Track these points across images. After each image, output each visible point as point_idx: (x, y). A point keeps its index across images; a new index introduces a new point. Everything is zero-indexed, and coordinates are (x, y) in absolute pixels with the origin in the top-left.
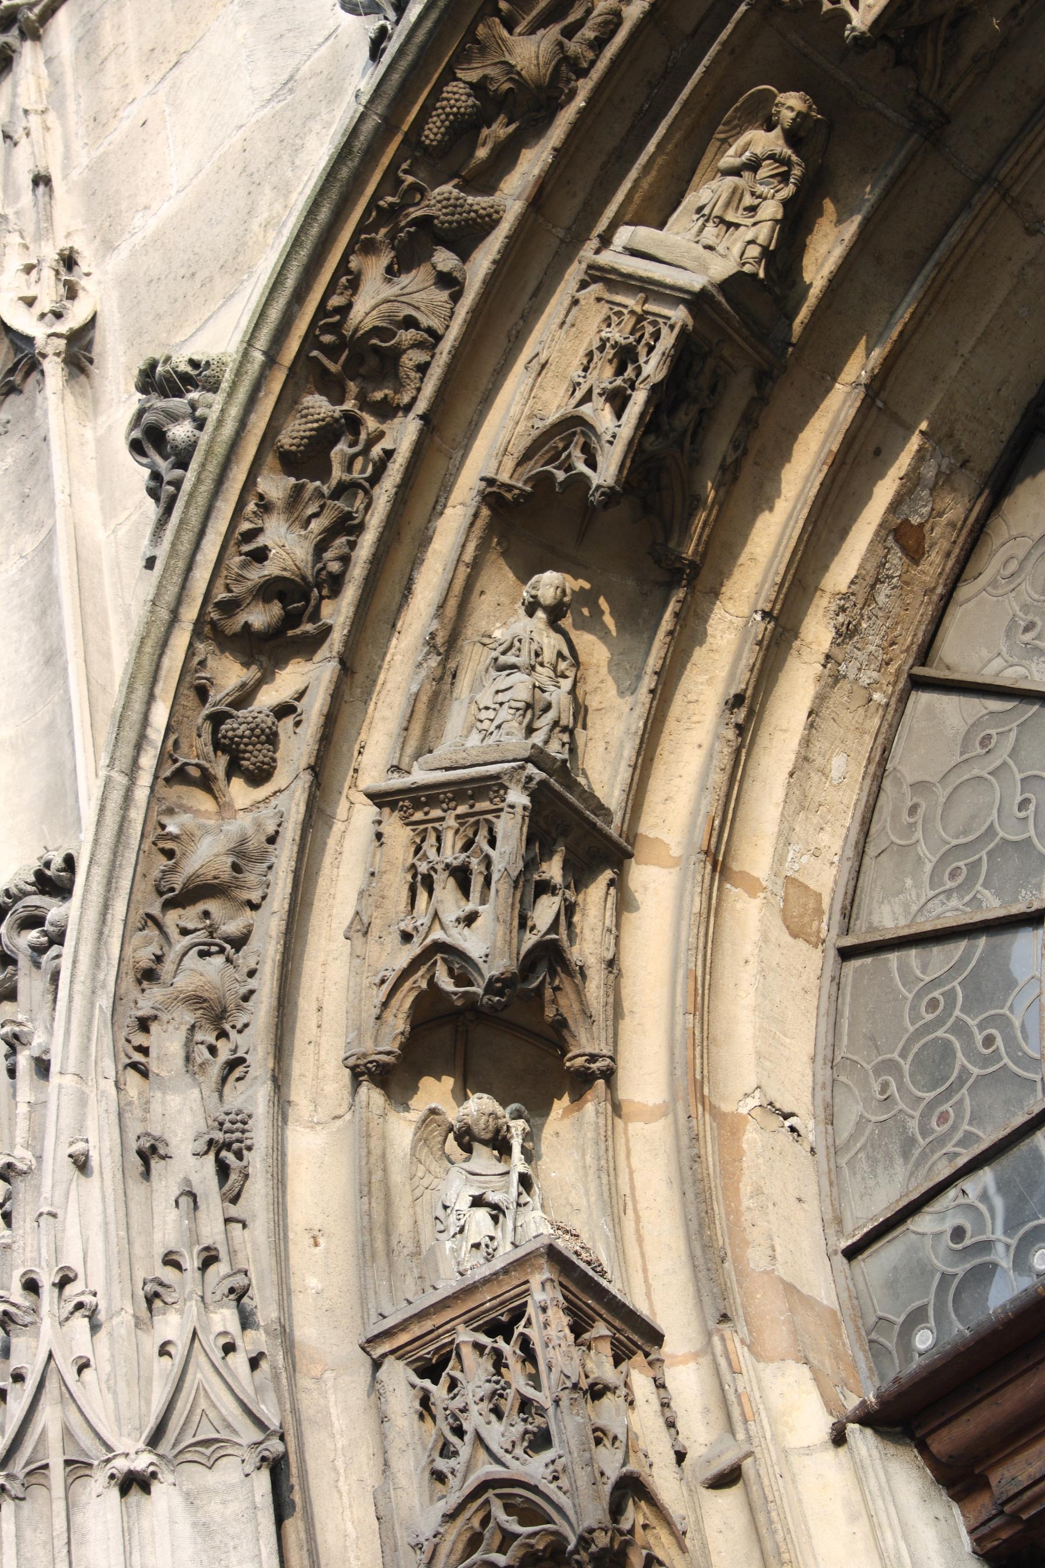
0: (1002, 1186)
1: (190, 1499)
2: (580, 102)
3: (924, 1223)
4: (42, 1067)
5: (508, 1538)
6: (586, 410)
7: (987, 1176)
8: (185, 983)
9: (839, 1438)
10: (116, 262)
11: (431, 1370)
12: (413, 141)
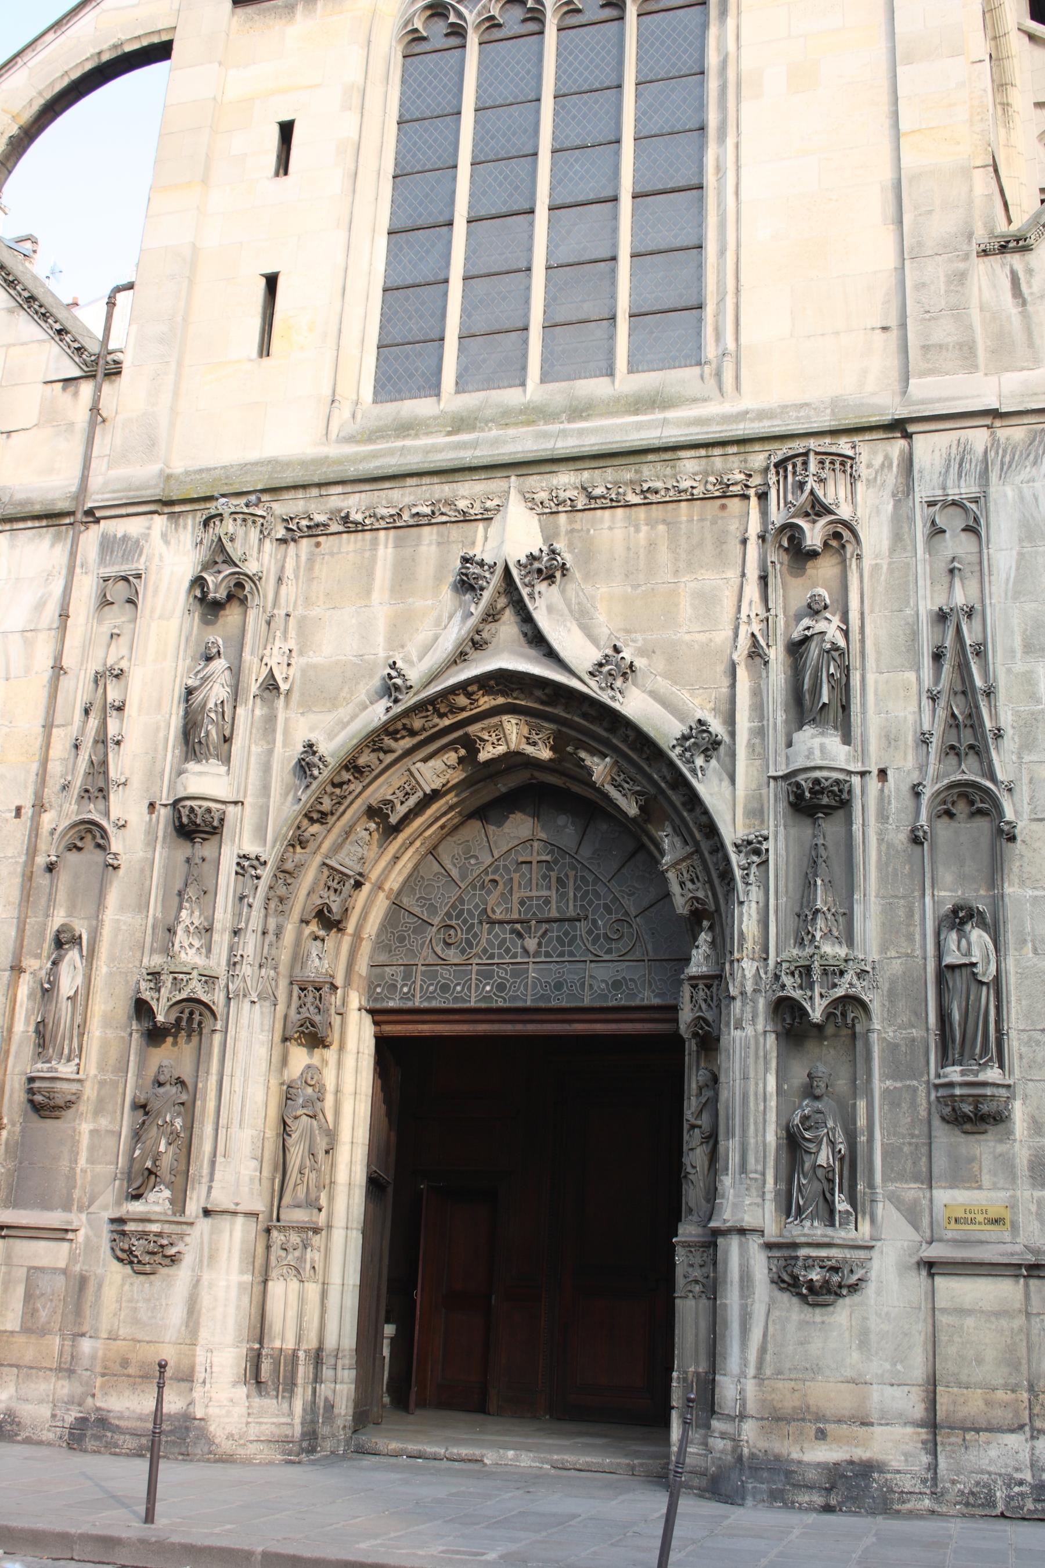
0: (404, 972)
1: (261, 1007)
2: (422, 737)
3: (387, 969)
4: (250, 906)
5: (307, 1028)
6: (395, 801)
7: (402, 968)
8: (279, 893)
9: (360, 1010)
10: (303, 661)
11: (302, 989)
12: (386, 730)
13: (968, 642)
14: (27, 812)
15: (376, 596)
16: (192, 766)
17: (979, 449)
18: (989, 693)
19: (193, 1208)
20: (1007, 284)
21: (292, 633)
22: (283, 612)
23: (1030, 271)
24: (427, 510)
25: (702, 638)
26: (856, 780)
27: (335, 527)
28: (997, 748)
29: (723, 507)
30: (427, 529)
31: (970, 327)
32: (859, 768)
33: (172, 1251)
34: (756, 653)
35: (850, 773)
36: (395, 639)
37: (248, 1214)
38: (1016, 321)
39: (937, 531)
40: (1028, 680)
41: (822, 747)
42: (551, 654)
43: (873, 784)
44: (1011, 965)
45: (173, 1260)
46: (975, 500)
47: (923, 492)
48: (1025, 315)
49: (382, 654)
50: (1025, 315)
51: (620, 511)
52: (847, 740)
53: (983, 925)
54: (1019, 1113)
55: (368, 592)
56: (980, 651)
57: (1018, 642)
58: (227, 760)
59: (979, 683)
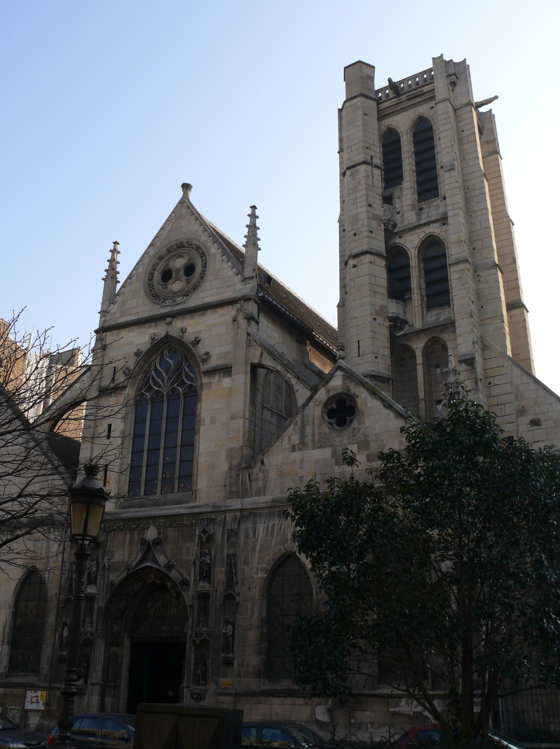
13: (233, 562)
14: (57, 594)
15: (126, 546)
16: (89, 586)
17: (238, 517)
18: (236, 573)
19: (89, 683)
20: (247, 476)
21: (110, 554)
22: (108, 549)
23: (252, 473)
24: (135, 527)
25: (186, 558)
26: (211, 592)
27: (118, 530)
28: (236, 586)
29: (192, 528)
30: (136, 531)
31: (239, 488)
32: (211, 589)
33: (84, 692)
34: (195, 563)
35: (209, 591)
36: (129, 557)
37: (100, 684)
38: (249, 485)
39: (229, 537)
40: (244, 570)
41: (203, 585)
42: (157, 563)
43: (215, 593)
44: (236, 632)
45: (85, 694)
46: (237, 529)
47: (227, 527)
48: (251, 484)
49: (127, 560)
50: (251, 484)
51: (173, 528)
52: (209, 583)
53: (231, 624)
54: (235, 662)
55: (124, 545)
56: (235, 564)
57: (243, 562)
58: (95, 584)
59: (234, 571)
